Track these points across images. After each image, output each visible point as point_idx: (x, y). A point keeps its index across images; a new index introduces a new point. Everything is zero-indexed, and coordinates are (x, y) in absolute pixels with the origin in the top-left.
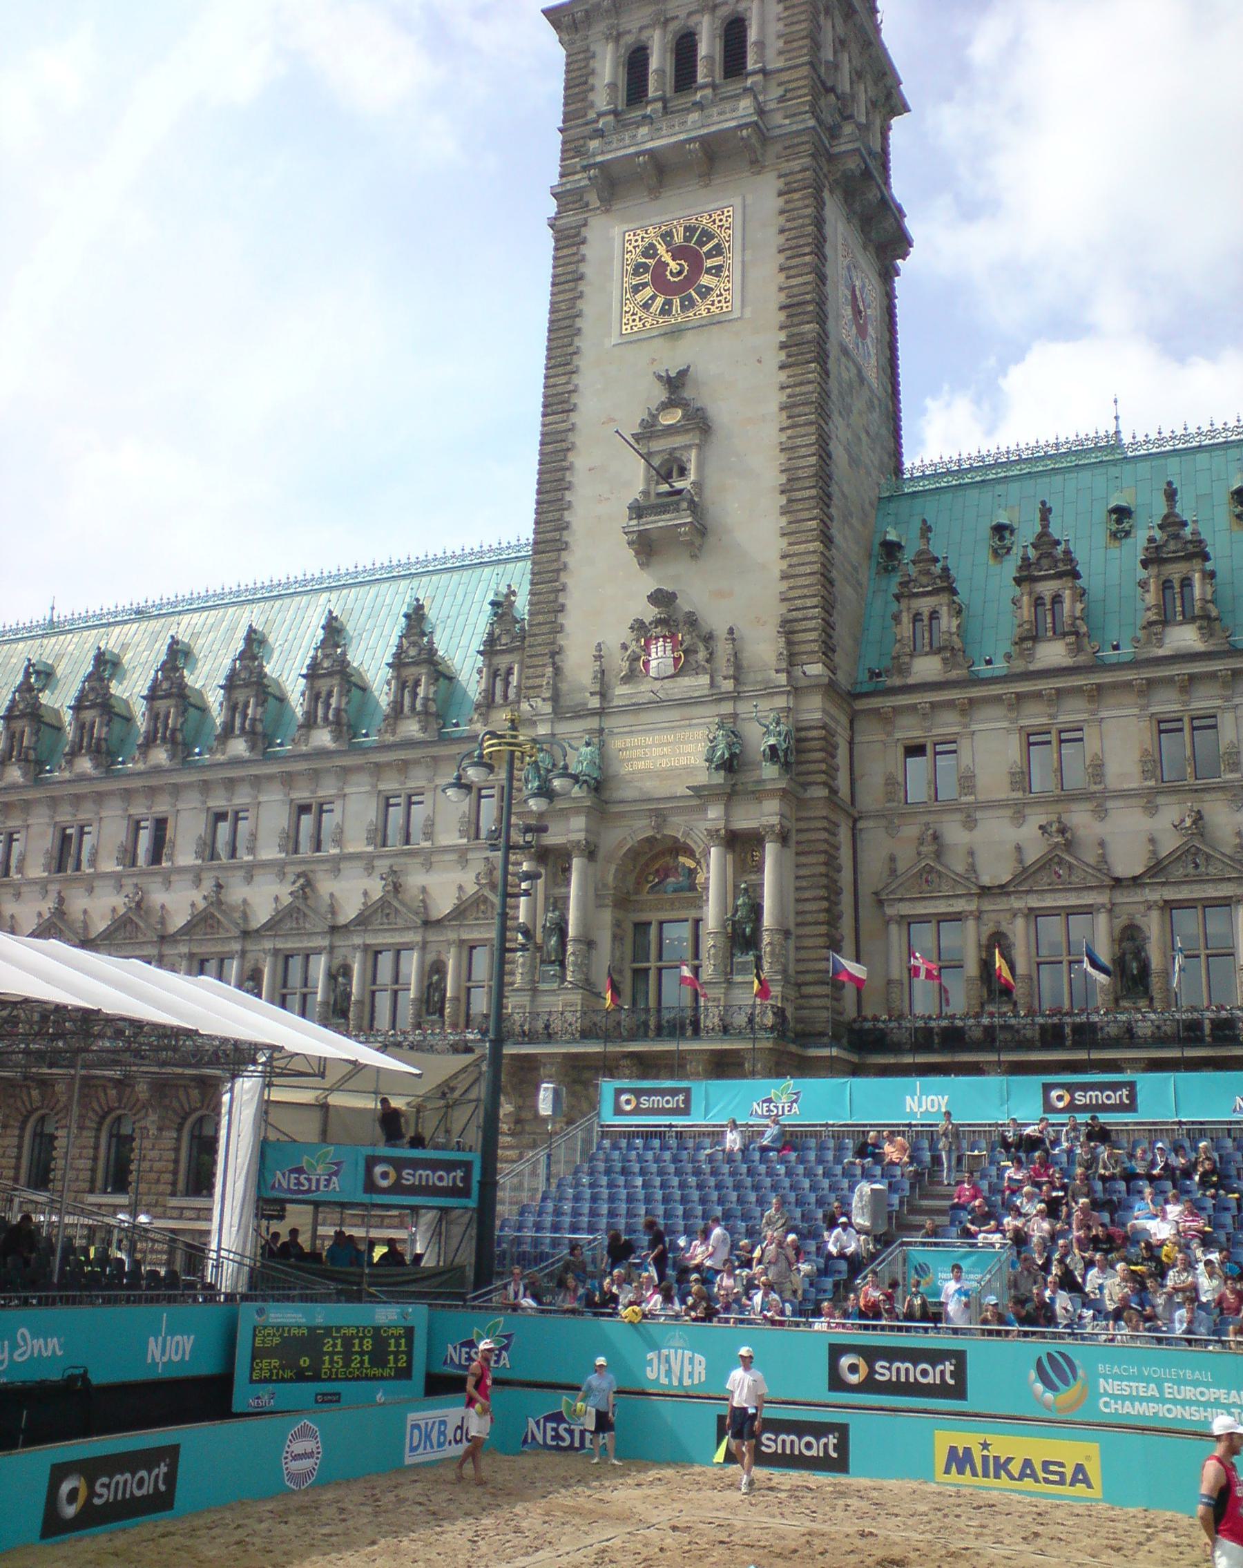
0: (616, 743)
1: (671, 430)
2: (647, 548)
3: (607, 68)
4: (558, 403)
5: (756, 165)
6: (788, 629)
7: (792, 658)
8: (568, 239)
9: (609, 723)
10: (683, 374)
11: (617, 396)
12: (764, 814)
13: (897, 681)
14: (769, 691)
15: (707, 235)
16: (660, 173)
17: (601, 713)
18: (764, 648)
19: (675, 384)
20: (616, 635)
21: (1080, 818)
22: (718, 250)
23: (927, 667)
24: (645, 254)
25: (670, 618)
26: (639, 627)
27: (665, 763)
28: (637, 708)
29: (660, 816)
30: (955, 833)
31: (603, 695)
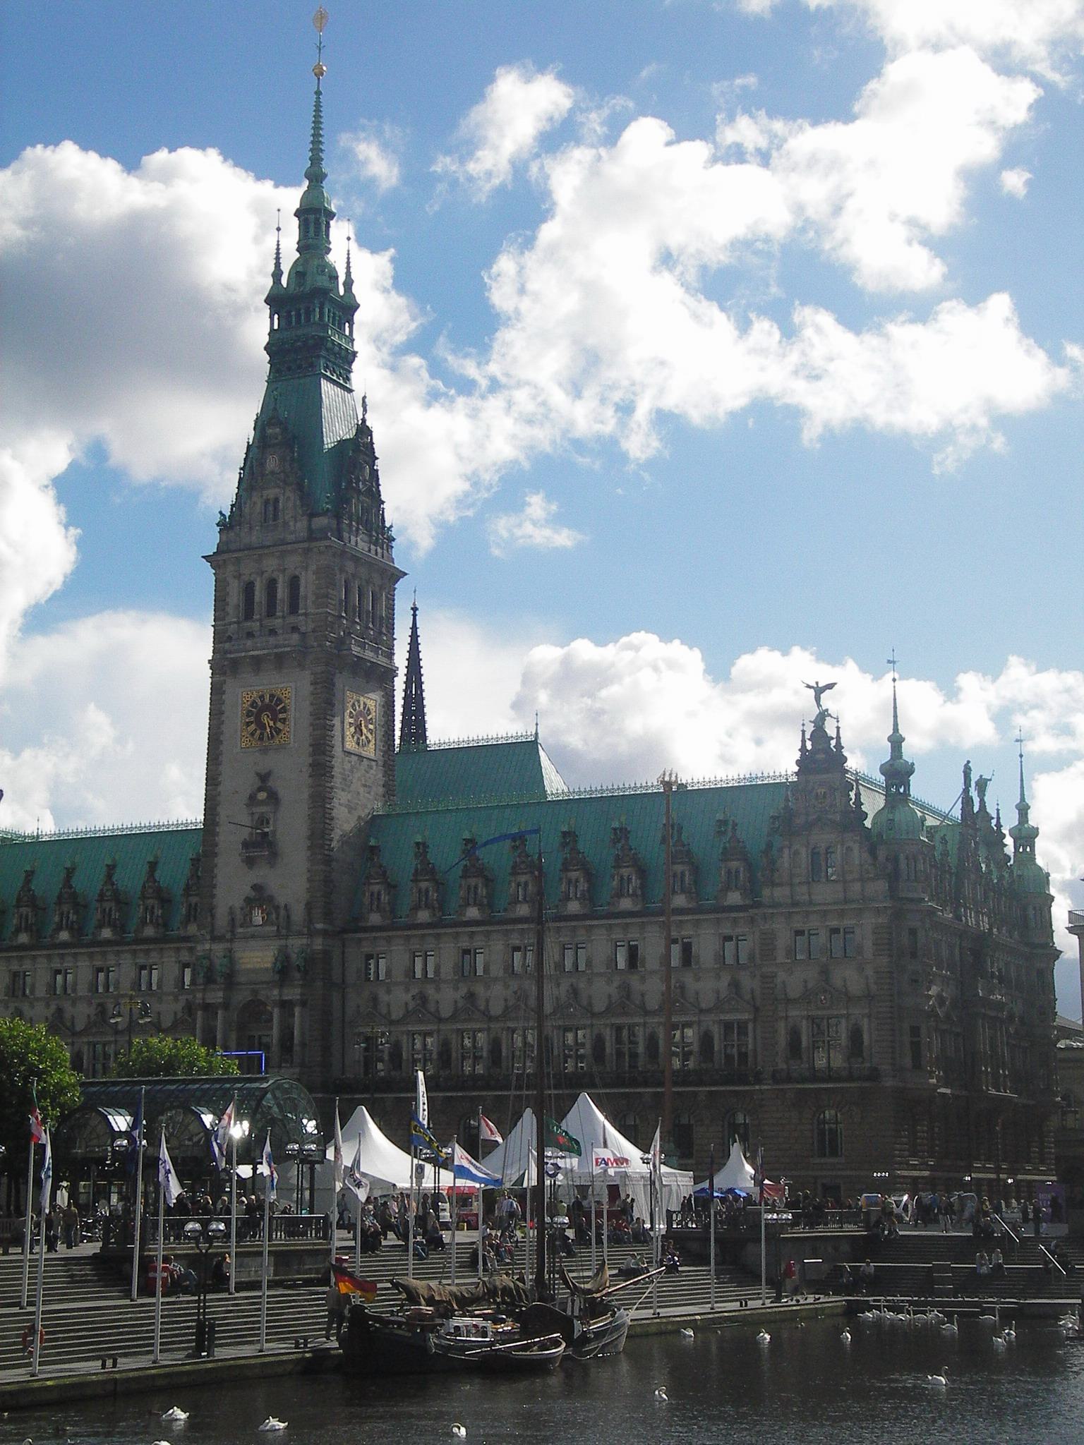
0: (238, 955)
1: (262, 803)
2: (250, 862)
3: (235, 597)
4: (212, 780)
5: (301, 666)
6: (309, 907)
7: (310, 921)
8: (217, 691)
9: (237, 945)
10: (269, 774)
11: (240, 782)
12: (293, 993)
13: (362, 924)
14: (300, 934)
15: (280, 701)
16: (257, 664)
17: (231, 941)
18: (298, 914)
19: (264, 778)
20: (238, 902)
21: (430, 991)
22: (284, 710)
23: (375, 919)
24: (252, 706)
25: (259, 897)
26: (248, 901)
27: (258, 966)
28: (246, 938)
29: (255, 992)
30: (384, 997)
31: (232, 932)
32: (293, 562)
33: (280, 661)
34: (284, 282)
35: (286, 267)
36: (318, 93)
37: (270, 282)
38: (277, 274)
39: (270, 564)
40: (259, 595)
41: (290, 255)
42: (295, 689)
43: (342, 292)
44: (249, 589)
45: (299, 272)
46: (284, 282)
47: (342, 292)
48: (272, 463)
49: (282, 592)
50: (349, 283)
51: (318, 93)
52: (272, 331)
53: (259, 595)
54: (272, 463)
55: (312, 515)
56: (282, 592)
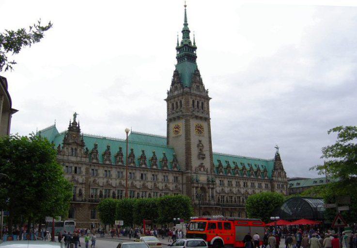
5: (183, 118)
16: (174, 119)
32: (180, 98)
33: (179, 118)
34: (180, 45)
35: (180, 43)
36: (185, 10)
37: (176, 45)
38: (178, 44)
39: (176, 99)
40: (175, 106)
41: (181, 39)
42: (181, 123)
43: (193, 45)
44: (173, 105)
45: (182, 43)
46: (180, 45)
47: (193, 45)
48: (175, 79)
49: (179, 104)
50: (194, 43)
51: (185, 10)
52: (177, 54)
53: (175, 106)
54: (175, 79)
55: (183, 88)
56: (179, 104)
